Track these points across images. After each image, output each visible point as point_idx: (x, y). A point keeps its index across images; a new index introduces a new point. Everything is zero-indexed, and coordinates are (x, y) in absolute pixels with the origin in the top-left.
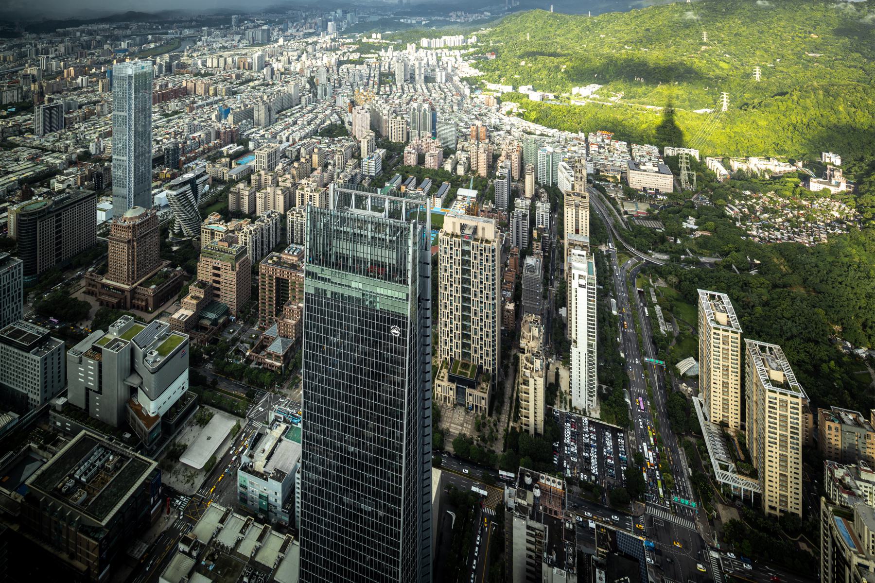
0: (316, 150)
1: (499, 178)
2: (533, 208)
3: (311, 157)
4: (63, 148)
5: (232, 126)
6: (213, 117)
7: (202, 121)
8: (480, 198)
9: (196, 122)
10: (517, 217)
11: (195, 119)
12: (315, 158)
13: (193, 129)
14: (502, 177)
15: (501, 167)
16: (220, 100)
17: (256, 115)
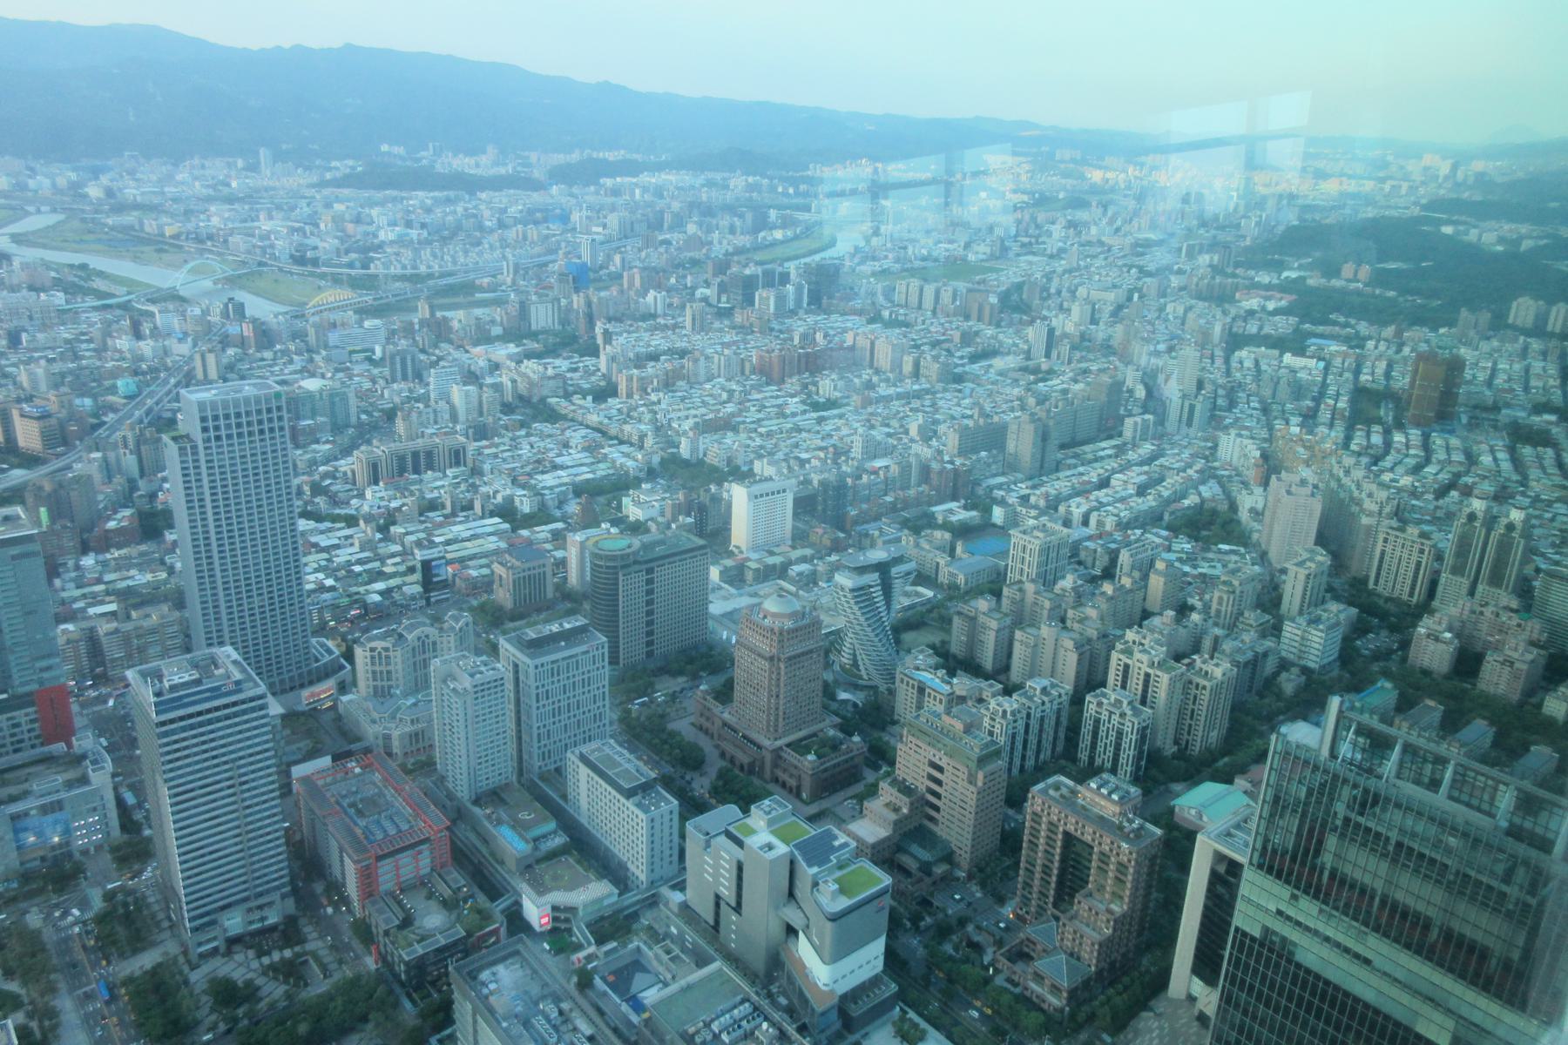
0: (1160, 565)
3: (1145, 577)
4: (635, 439)
5: (958, 462)
12: (1156, 583)
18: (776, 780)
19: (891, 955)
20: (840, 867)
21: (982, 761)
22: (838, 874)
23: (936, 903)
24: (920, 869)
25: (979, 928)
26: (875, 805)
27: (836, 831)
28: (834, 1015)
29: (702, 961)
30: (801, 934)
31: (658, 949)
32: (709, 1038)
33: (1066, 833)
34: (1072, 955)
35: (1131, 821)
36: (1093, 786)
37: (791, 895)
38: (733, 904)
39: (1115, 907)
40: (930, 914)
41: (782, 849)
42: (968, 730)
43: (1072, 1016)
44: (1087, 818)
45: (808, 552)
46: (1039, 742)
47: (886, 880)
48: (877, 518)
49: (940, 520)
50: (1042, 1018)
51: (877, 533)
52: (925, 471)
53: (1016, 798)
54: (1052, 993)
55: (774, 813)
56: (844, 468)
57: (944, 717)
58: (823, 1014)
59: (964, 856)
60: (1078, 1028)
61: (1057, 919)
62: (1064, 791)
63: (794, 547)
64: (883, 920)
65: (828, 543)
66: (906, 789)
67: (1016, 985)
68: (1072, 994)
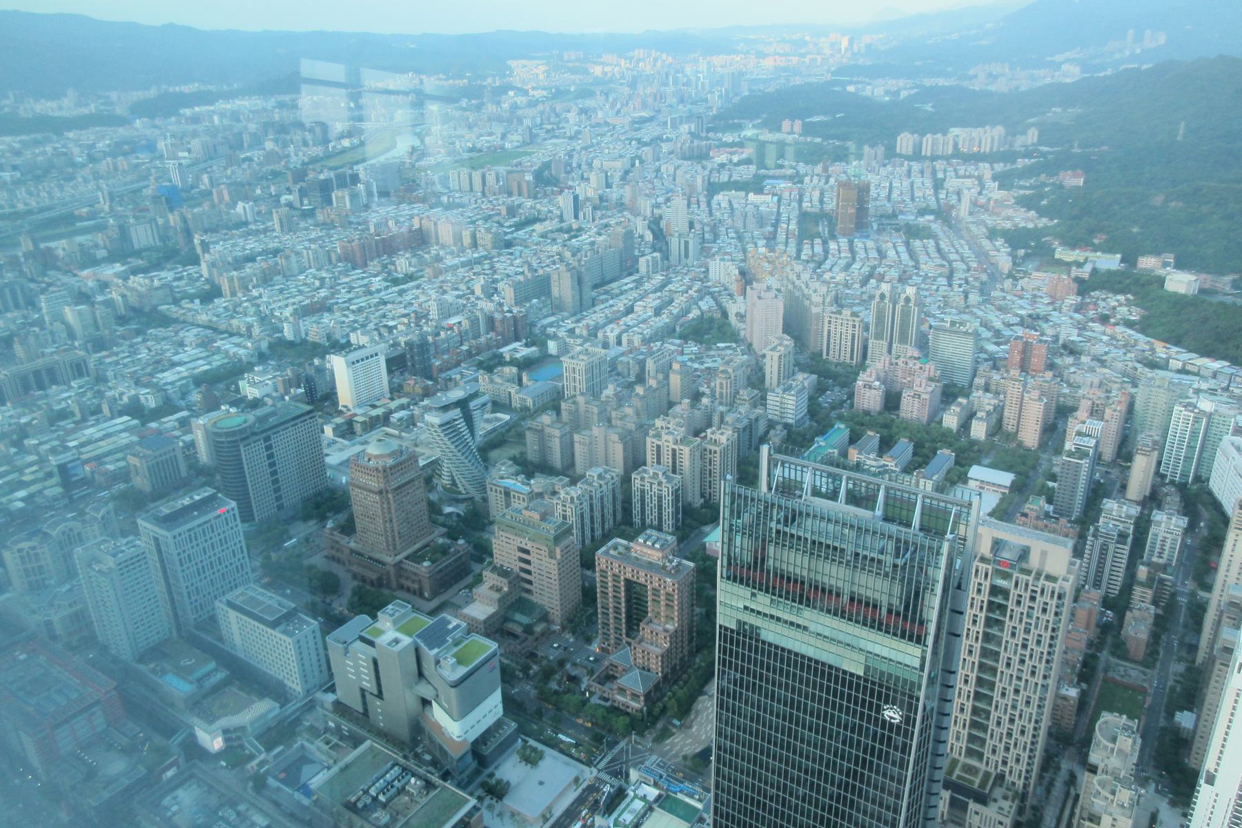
0: (676, 366)
1: (1070, 454)
2: (1142, 526)
3: (667, 377)
5: (515, 310)
6: (478, 292)
7: (458, 297)
8: (1020, 489)
9: (449, 297)
10: (1107, 536)
11: (445, 292)
12: (675, 380)
13: (446, 311)
14: (1080, 453)
15: (1079, 434)
16: (486, 258)
17: (555, 292)
18: (401, 587)
19: (507, 700)
20: (456, 645)
21: (557, 539)
22: (456, 650)
23: (540, 654)
24: (524, 631)
25: (575, 664)
26: (483, 590)
27: (449, 617)
28: (469, 758)
29: (356, 742)
30: (434, 703)
31: (319, 743)
32: (369, 801)
33: (626, 580)
34: (643, 668)
35: (671, 561)
36: (641, 541)
37: (421, 675)
38: (376, 692)
39: (669, 627)
40: (535, 663)
41: (406, 640)
42: (543, 518)
43: (650, 712)
44: (641, 566)
45: (405, 400)
46: (603, 515)
47: (493, 646)
48: (458, 364)
49: (508, 359)
50: (628, 720)
51: (458, 377)
52: (491, 321)
53: (588, 563)
54: (633, 699)
55: (397, 614)
56: (425, 329)
57: (524, 512)
58: (461, 758)
59: (557, 614)
60: (655, 720)
61: (629, 644)
62: (621, 549)
63: (392, 399)
64: (497, 674)
65: (419, 390)
66: (503, 573)
67: (606, 700)
68: (647, 696)
